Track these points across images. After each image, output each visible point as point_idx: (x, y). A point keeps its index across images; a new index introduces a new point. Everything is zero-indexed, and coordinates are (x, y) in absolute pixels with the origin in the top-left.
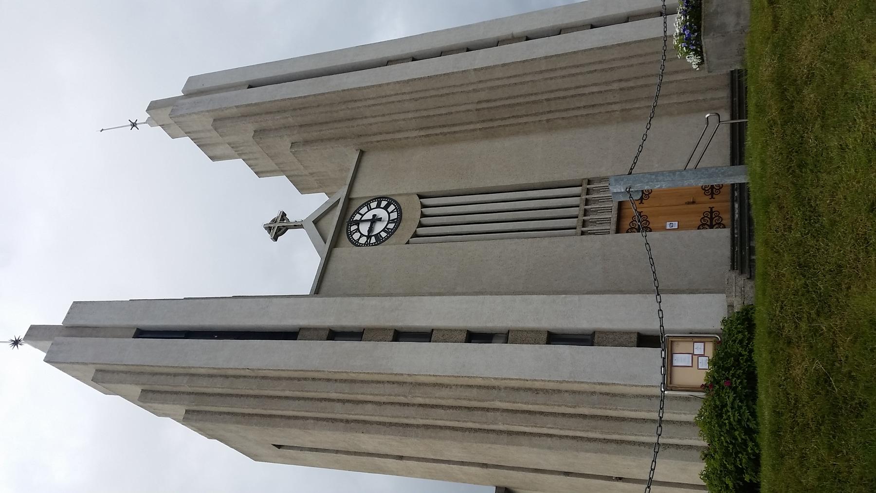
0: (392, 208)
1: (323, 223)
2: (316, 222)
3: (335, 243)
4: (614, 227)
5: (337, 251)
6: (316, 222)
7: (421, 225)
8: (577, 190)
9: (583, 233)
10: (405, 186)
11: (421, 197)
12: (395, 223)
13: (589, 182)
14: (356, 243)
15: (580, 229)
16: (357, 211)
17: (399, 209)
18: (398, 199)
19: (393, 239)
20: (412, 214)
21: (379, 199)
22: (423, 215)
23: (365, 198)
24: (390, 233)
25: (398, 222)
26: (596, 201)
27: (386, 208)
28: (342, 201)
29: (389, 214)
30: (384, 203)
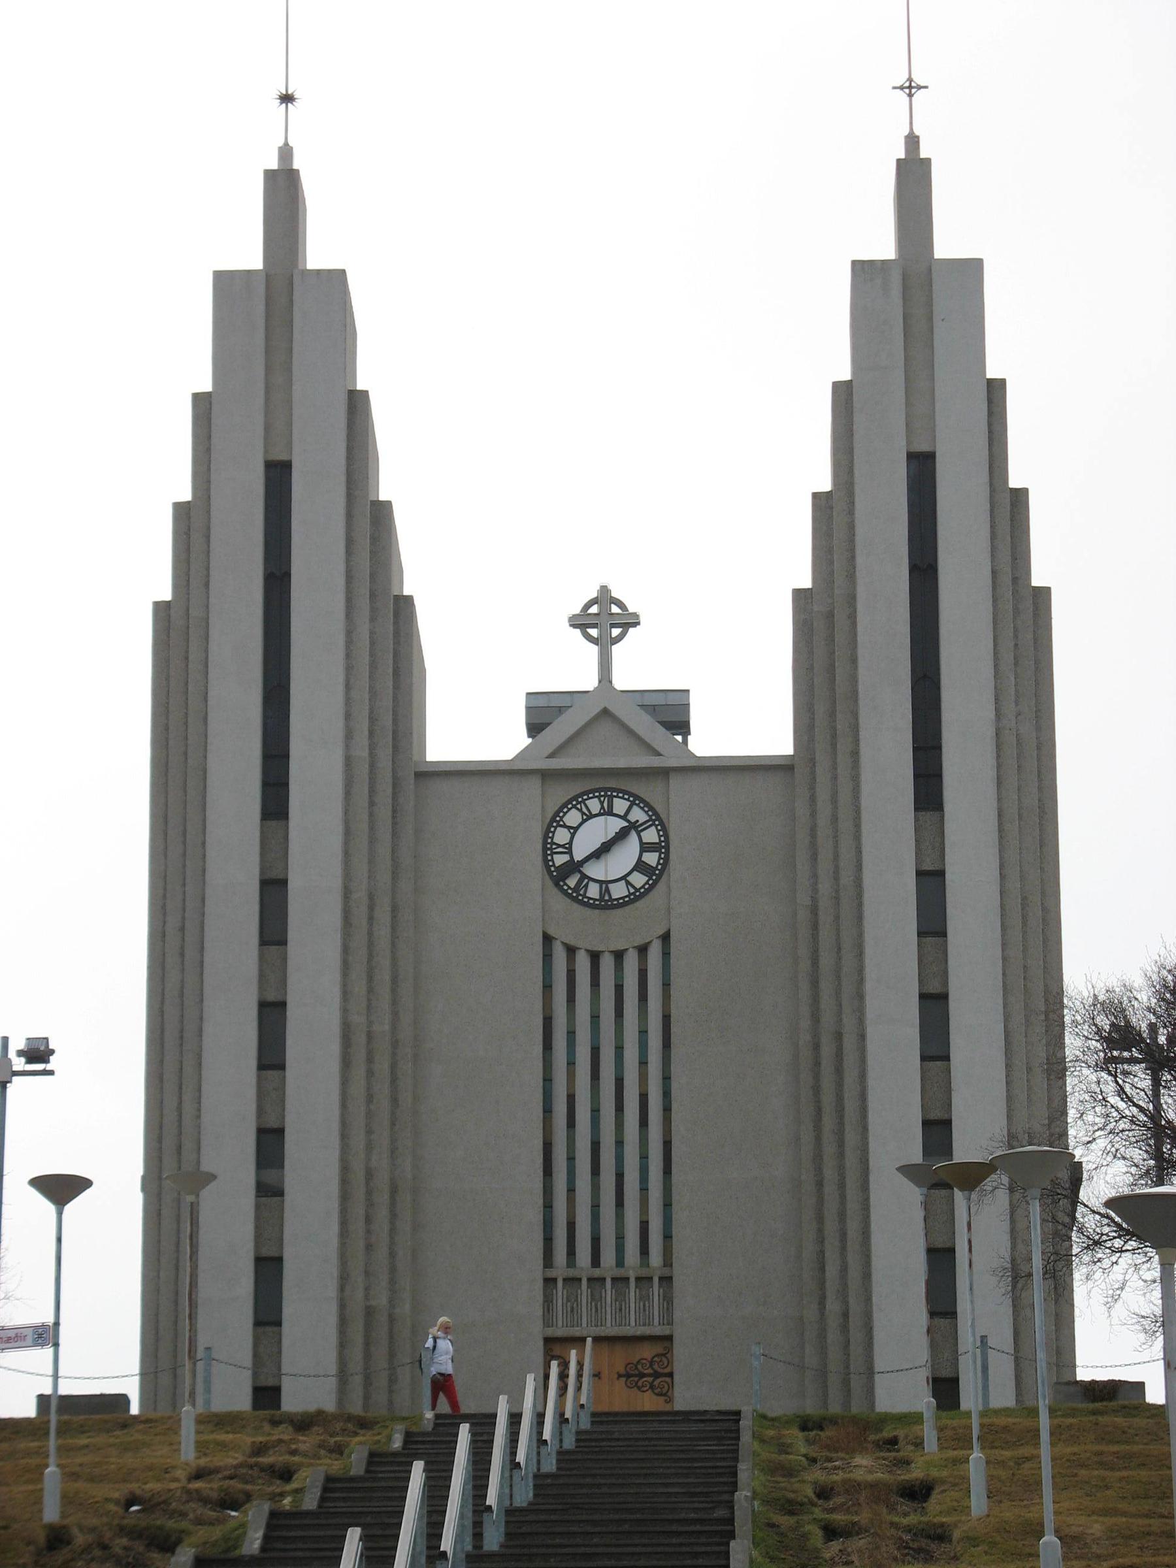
0: (639, 880)
1: (605, 729)
2: (605, 712)
3: (547, 776)
4: (560, 1332)
5: (533, 787)
6: (605, 712)
7: (595, 957)
8: (656, 1258)
9: (549, 1282)
10: (687, 903)
11: (666, 938)
12: (602, 898)
13: (667, 1280)
14: (555, 821)
15: (551, 1273)
16: (636, 800)
17: (636, 896)
18: (661, 886)
19: (558, 902)
20: (620, 932)
21: (662, 847)
22: (619, 956)
23: (668, 815)
24: (577, 897)
25: (606, 904)
26: (620, 1297)
27: (640, 866)
28: (655, 762)
29: (624, 878)
30: (651, 858)
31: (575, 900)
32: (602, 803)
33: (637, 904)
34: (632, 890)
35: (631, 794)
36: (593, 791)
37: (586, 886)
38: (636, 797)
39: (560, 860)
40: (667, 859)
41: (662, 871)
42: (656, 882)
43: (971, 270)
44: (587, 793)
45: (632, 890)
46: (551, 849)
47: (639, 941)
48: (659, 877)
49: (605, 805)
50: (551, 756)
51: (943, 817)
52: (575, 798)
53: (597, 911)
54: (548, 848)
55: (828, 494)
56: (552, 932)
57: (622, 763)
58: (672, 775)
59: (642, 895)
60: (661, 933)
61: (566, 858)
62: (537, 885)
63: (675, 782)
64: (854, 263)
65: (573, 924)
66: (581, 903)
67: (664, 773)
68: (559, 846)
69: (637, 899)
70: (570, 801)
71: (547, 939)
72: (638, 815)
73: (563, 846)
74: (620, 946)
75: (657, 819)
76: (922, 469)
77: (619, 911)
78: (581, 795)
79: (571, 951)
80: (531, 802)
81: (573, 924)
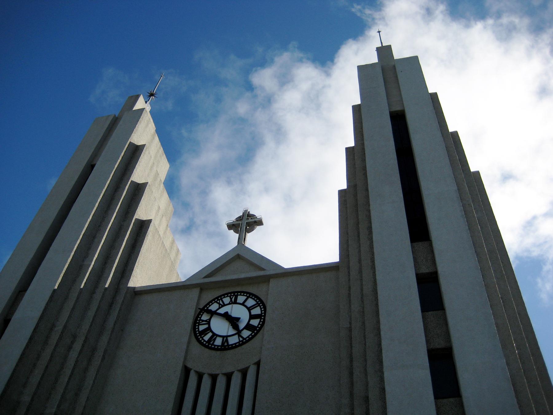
16: (250, 295)
17: (243, 342)
18: (259, 336)
20: (230, 362)
22: (229, 377)
24: (209, 345)
28: (261, 273)
31: (207, 347)
32: (231, 299)
33: (244, 346)
34: (241, 339)
35: (247, 293)
36: (227, 294)
37: (215, 339)
38: (250, 294)
39: (202, 328)
40: (264, 322)
41: (260, 328)
42: (256, 334)
43: (413, 63)
44: (224, 295)
45: (241, 339)
46: (199, 323)
47: (242, 366)
48: (258, 331)
49: (233, 300)
50: (205, 277)
51: (431, 245)
52: (217, 298)
53: (219, 352)
54: (197, 321)
55: (353, 147)
56: (189, 365)
57: (243, 276)
58: (271, 280)
59: (247, 341)
60: (256, 360)
61: (206, 326)
62: (185, 339)
63: (273, 283)
64: (358, 67)
65: (202, 360)
66: (210, 348)
67: (266, 279)
68: (203, 321)
69: (243, 343)
70: (214, 300)
71: (187, 371)
72: (251, 302)
73: (206, 321)
74: (229, 370)
75: (260, 303)
76: (399, 121)
77: (232, 351)
78: (221, 296)
79: (200, 376)
80: (191, 302)
81: (202, 360)
